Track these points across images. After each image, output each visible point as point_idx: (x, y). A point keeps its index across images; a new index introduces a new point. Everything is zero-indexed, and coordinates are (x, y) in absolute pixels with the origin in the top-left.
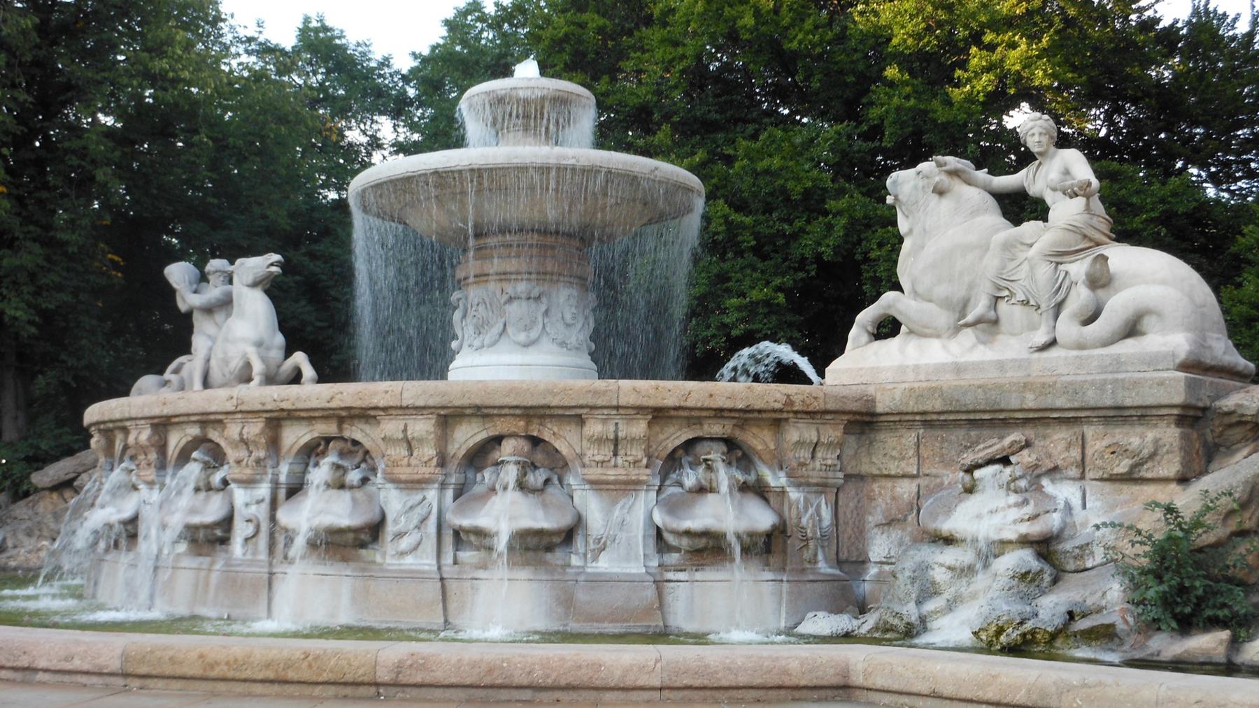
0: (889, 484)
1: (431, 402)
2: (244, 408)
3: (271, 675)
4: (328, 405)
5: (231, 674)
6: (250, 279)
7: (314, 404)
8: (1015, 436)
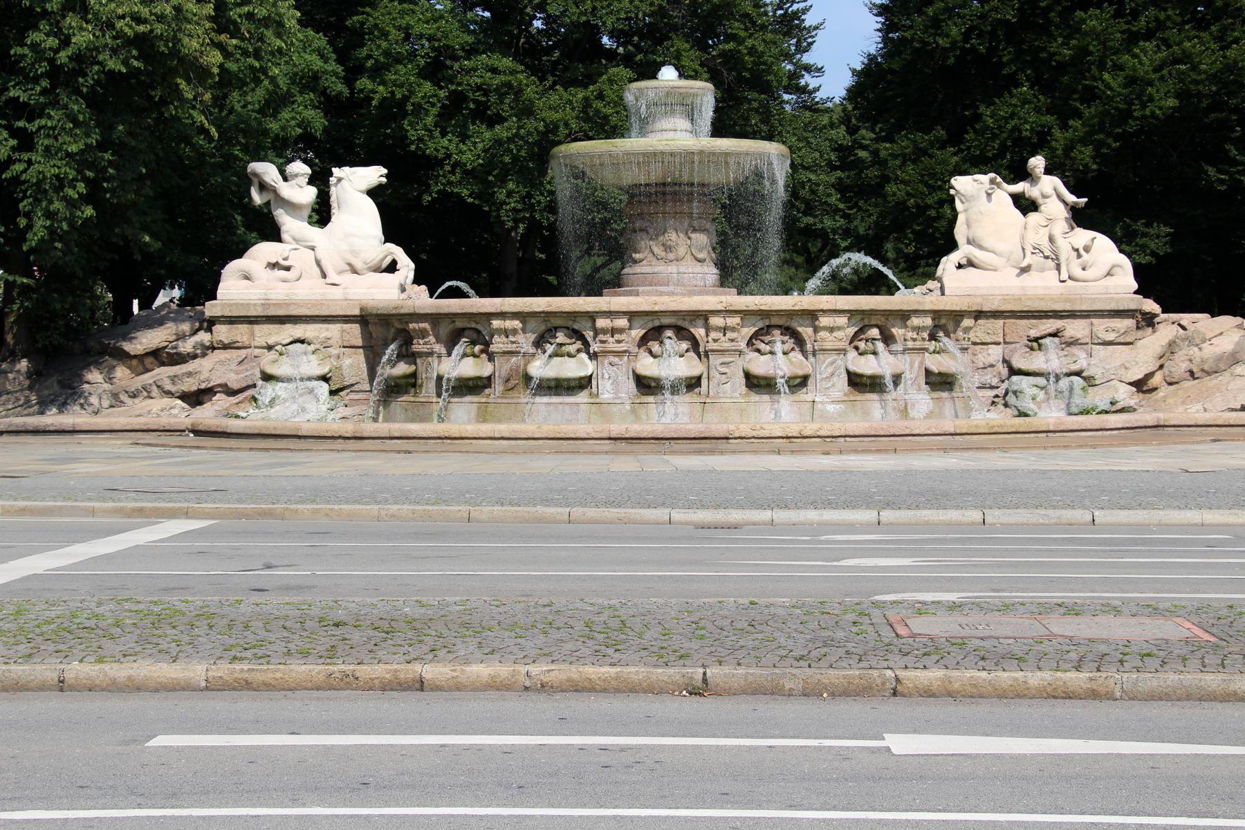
0: (985, 347)
1: (852, 308)
2: (731, 308)
3: (1014, 430)
4: (792, 308)
5: (1000, 430)
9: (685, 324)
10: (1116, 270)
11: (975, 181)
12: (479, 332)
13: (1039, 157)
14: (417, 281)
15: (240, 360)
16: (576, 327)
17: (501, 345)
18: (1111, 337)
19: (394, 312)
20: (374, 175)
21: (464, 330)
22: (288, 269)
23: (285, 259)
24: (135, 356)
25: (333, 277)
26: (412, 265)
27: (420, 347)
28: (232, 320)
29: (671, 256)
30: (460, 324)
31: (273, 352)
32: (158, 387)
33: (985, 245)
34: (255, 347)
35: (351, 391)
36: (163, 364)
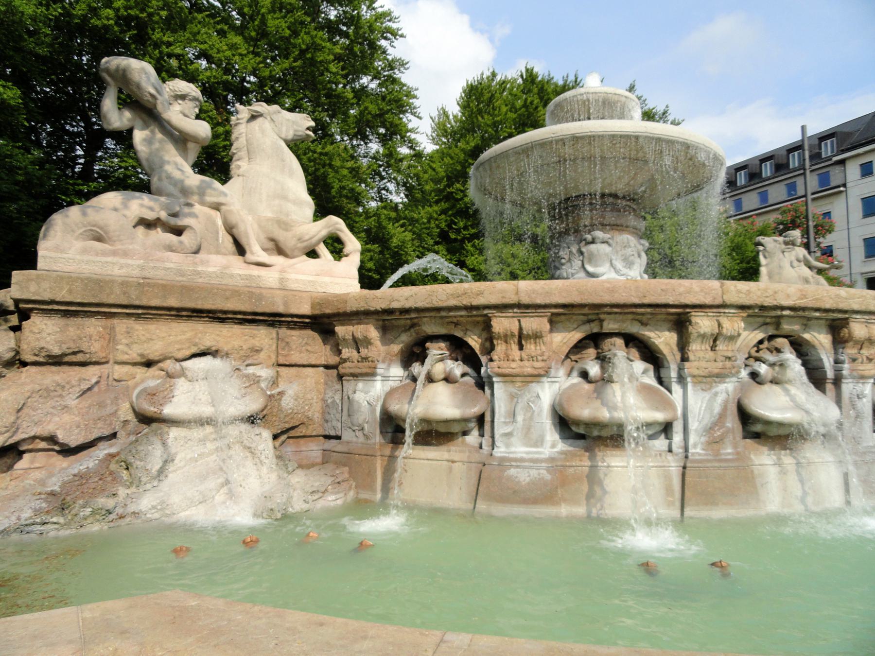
6: (290, 136)
11: (775, 241)
15: (85, 387)
17: (703, 364)
19: (452, 302)
22: (178, 231)
25: (256, 252)
27: (514, 365)
31: (153, 371)
34: (117, 363)
35: (289, 438)
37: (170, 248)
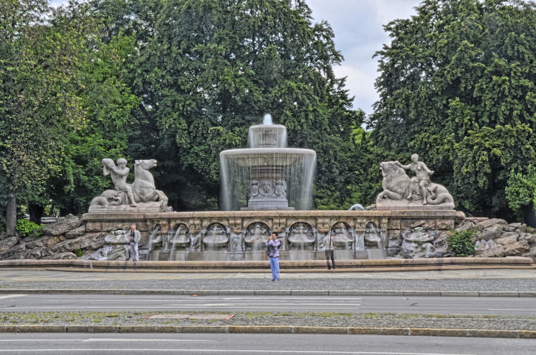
6: (147, 167)
7: (303, 215)
8: (422, 222)
9: (264, 222)
10: (447, 200)
12: (185, 225)
13: (416, 154)
14: (169, 205)
16: (222, 223)
18: (444, 227)
20: (152, 162)
21: (180, 224)
22: (116, 200)
23: (116, 196)
24: (56, 236)
25: (134, 203)
26: (167, 198)
28: (94, 221)
29: (267, 195)
30: (178, 222)
32: (64, 248)
33: (394, 190)
36: (67, 238)
37: (114, 205)
